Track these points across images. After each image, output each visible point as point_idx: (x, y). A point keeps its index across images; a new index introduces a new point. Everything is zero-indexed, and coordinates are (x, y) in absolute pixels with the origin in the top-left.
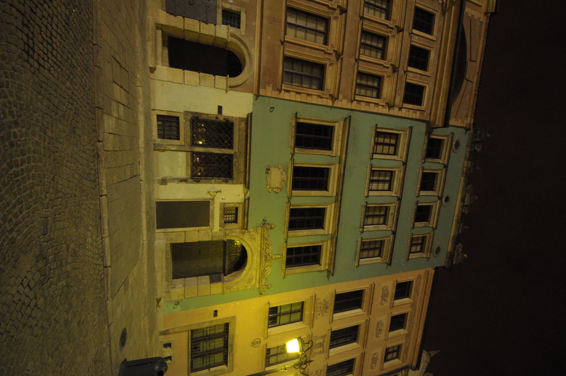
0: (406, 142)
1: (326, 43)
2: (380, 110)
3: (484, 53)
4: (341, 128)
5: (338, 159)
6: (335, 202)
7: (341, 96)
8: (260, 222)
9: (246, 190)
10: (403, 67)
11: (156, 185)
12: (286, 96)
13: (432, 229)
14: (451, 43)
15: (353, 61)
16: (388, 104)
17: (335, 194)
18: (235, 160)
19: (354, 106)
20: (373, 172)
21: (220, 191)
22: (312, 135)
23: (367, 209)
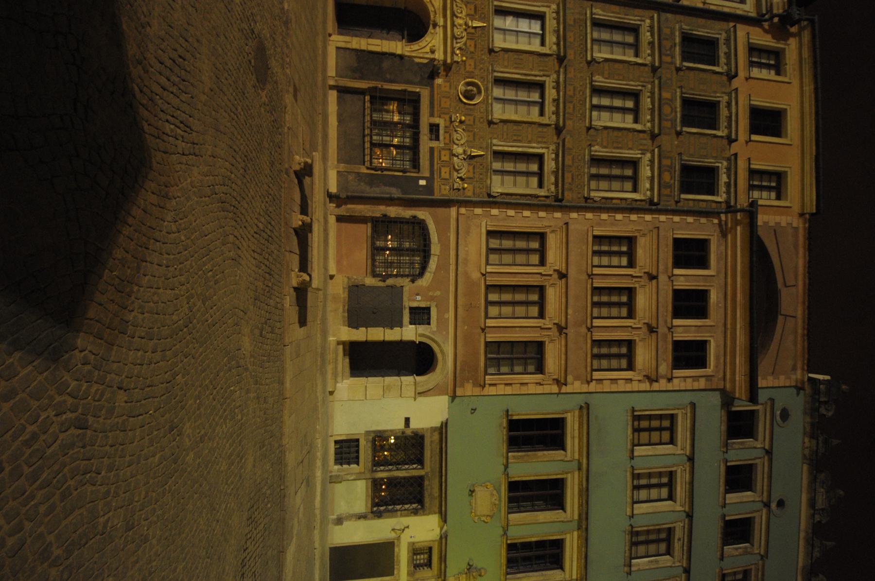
0: (689, 425)
2: (635, 386)
3: (809, 273)
4: (577, 419)
5: (575, 464)
6: (579, 529)
7: (570, 378)
8: (465, 566)
9: (442, 523)
10: (666, 321)
11: (330, 526)
12: (492, 391)
13: (759, 557)
14: (742, 277)
15: (583, 330)
16: (648, 377)
17: (576, 517)
18: (426, 483)
19: (593, 387)
20: (636, 476)
21: (408, 527)
22: (532, 433)
23: (633, 533)
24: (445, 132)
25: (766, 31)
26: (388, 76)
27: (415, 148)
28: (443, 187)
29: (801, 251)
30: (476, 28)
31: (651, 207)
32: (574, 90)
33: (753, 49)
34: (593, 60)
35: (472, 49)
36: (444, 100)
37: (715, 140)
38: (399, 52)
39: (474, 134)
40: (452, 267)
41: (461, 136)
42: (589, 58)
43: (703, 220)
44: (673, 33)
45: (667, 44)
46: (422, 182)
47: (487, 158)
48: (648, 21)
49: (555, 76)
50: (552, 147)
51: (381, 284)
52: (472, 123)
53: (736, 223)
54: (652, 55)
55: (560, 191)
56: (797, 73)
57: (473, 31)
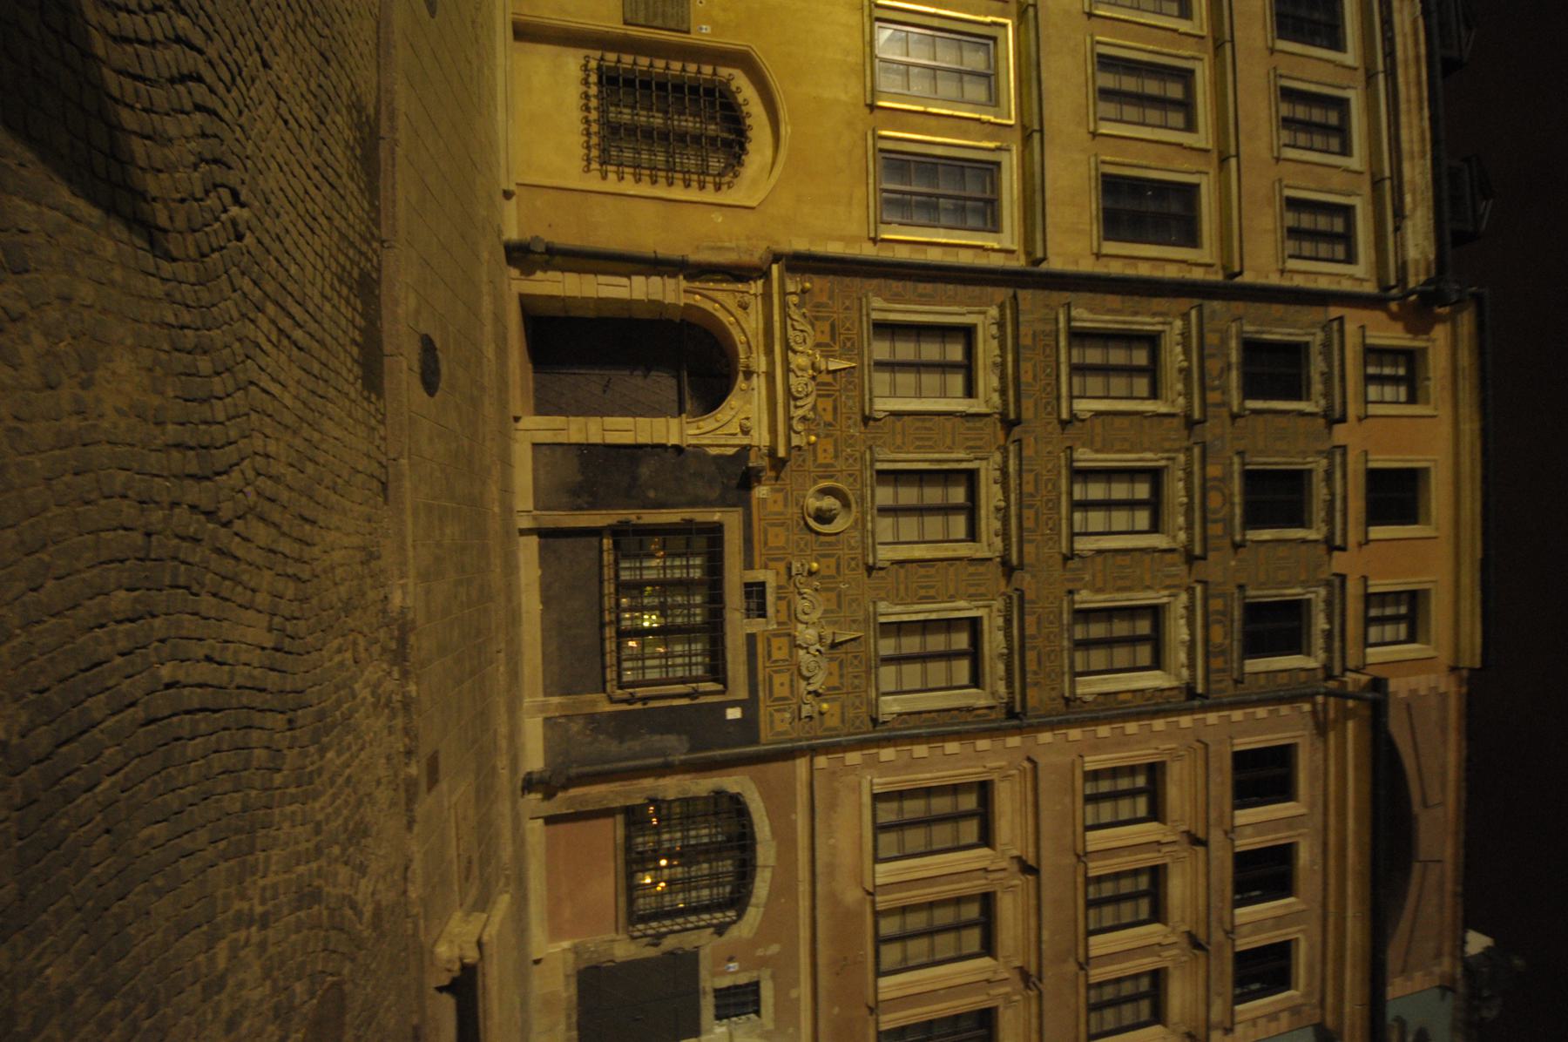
1: (970, 392)
10: (1221, 921)
14: (1358, 819)
15: (1071, 967)
24: (780, 598)
25: (1394, 317)
26: (652, 494)
27: (714, 629)
28: (777, 716)
29: (1452, 737)
30: (835, 371)
31: (1190, 698)
32: (1036, 481)
33: (1373, 353)
34: (1074, 417)
35: (829, 417)
36: (772, 531)
37: (1304, 547)
38: (674, 440)
39: (839, 596)
40: (804, 888)
41: (811, 605)
43: (1284, 710)
44: (1224, 341)
45: (1214, 366)
46: (734, 714)
47: (867, 643)
48: (1178, 323)
49: (998, 457)
50: (998, 604)
51: (651, 952)
52: (833, 572)
53: (1345, 715)
54: (1188, 394)
55: (1018, 697)
56: (1447, 395)
57: (828, 379)
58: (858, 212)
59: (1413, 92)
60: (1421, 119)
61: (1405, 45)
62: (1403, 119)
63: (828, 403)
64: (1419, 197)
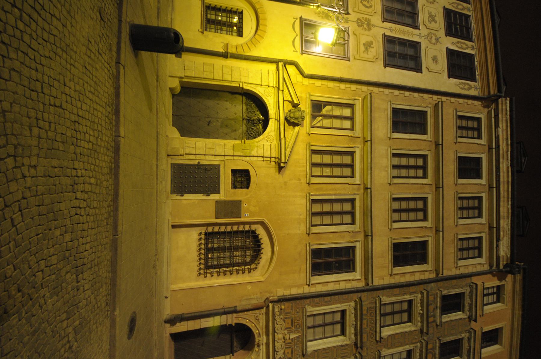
42: (378, 339)
44: (435, 298)
48: (420, 296)
56: (511, 300)
58: (303, 275)
59: (506, 193)
60: (508, 205)
61: (504, 177)
62: (501, 204)
63: (289, 351)
64: (505, 233)
